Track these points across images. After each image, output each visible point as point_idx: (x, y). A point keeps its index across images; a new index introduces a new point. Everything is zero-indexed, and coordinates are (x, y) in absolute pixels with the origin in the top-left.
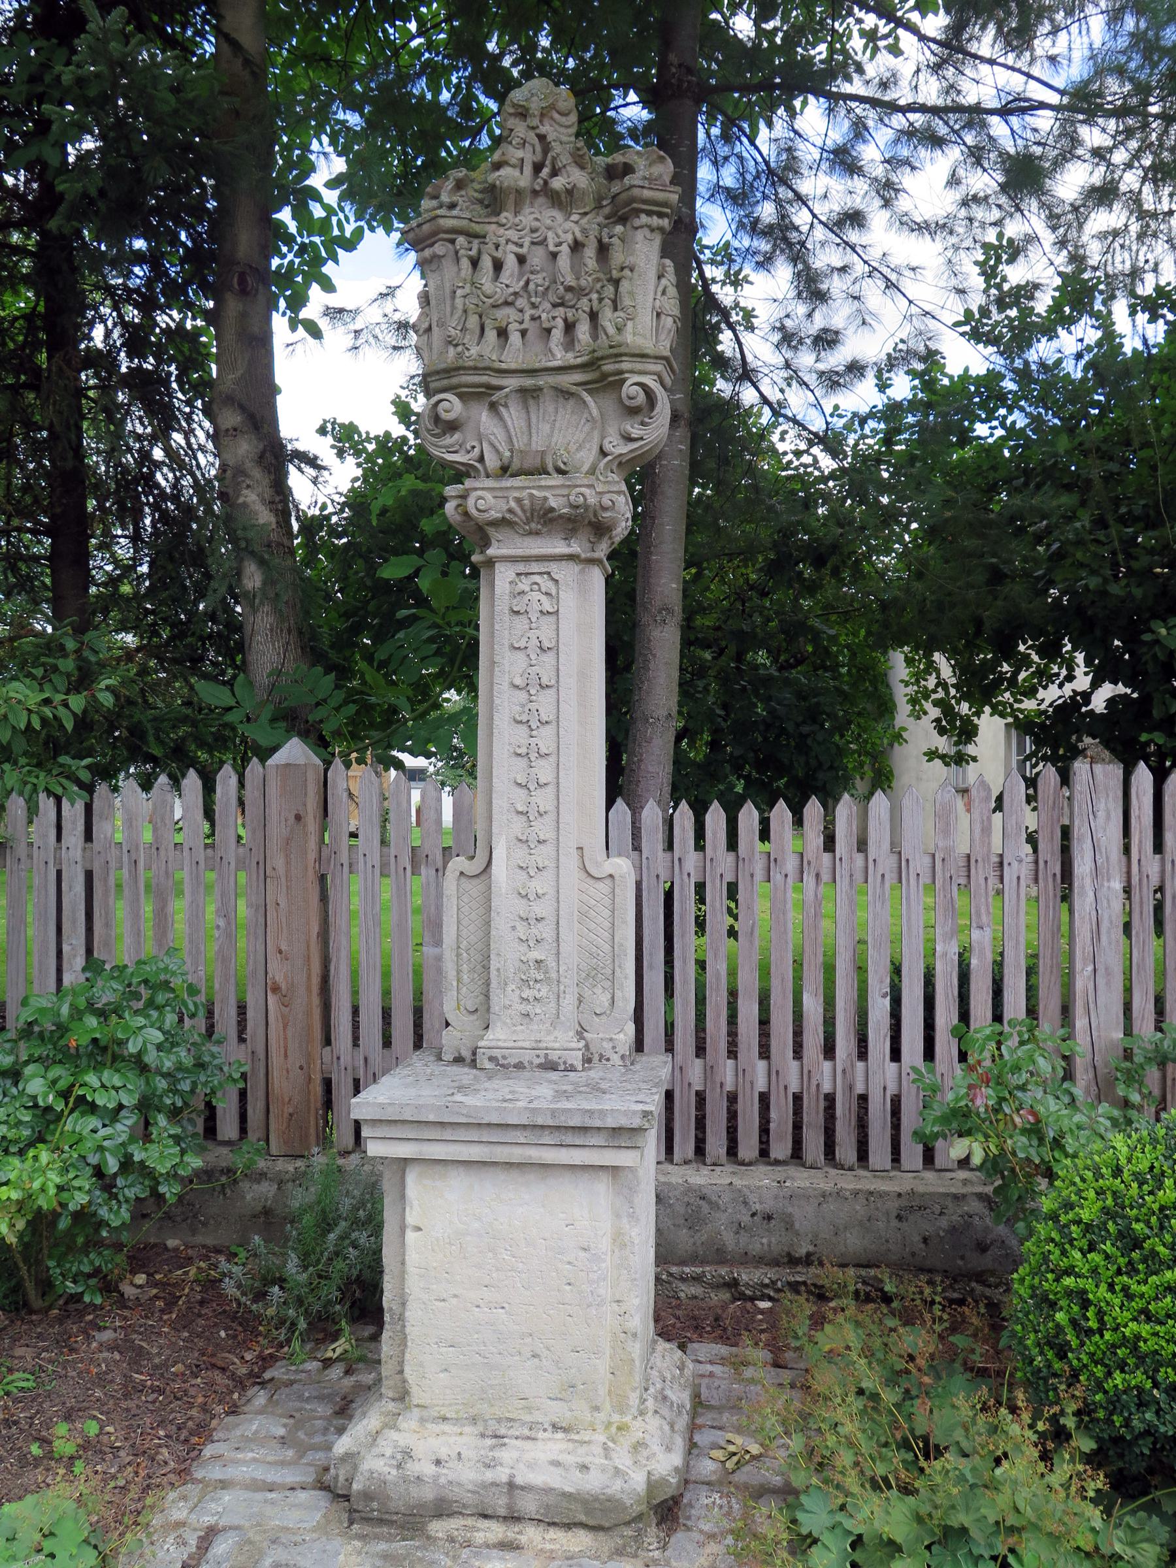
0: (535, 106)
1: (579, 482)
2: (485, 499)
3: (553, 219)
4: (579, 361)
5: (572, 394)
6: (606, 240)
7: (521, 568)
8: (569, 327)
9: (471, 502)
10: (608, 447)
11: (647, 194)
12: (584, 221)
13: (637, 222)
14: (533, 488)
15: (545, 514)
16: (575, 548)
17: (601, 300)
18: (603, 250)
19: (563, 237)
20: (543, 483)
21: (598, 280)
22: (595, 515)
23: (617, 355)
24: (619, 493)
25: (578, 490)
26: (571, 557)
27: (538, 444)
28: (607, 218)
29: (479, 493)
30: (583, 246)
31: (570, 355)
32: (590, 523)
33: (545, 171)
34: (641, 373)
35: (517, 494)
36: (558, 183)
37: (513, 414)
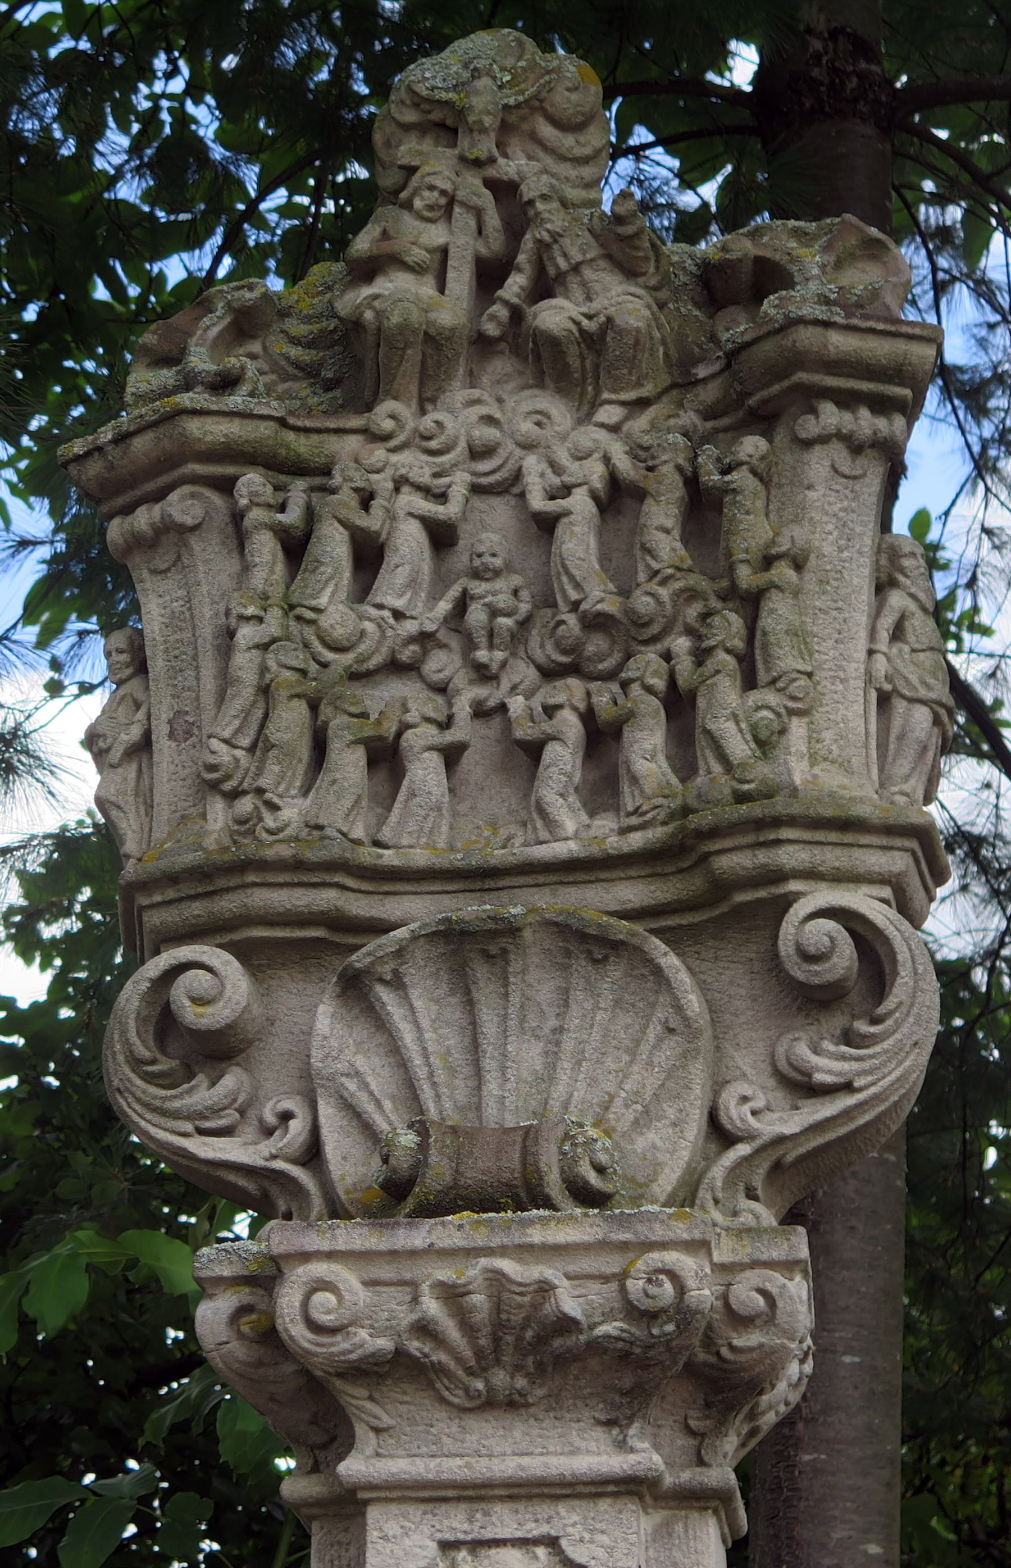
0: (484, 101)
1: (658, 1233)
2: (343, 1290)
3: (542, 420)
4: (636, 840)
5: (616, 946)
6: (712, 477)
7: (456, 1522)
8: (602, 738)
9: (289, 1300)
10: (735, 1114)
11: (840, 342)
12: (641, 423)
13: (809, 427)
14: (503, 1251)
15: (542, 1340)
16: (644, 1455)
17: (701, 655)
18: (704, 508)
19: (575, 470)
20: (536, 1236)
21: (692, 595)
22: (709, 1341)
23: (760, 824)
24: (788, 1266)
25: (656, 1258)
26: (633, 1488)
27: (505, 1104)
28: (709, 414)
29: (319, 1269)
30: (640, 494)
31: (605, 824)
32: (691, 1369)
33: (515, 285)
34: (839, 878)
35: (445, 1274)
36: (555, 316)
37: (422, 1014)
